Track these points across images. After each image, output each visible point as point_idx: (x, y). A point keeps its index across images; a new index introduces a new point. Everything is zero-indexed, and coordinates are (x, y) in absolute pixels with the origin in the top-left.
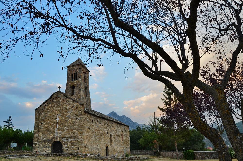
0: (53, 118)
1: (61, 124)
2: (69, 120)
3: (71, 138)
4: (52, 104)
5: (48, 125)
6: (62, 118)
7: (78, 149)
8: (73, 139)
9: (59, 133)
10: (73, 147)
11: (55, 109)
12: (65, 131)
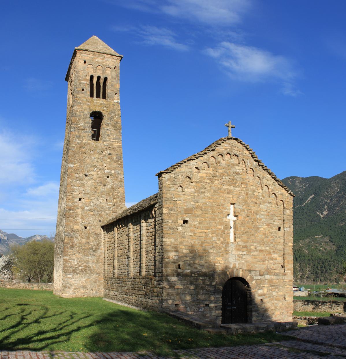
0: (222, 213)
1: (243, 234)
2: (263, 228)
3: (269, 271)
4: (215, 170)
5: (206, 231)
6: (246, 218)
7: (285, 298)
8: (273, 275)
9: (240, 256)
10: (274, 294)
11: (224, 187)
12: (255, 253)
